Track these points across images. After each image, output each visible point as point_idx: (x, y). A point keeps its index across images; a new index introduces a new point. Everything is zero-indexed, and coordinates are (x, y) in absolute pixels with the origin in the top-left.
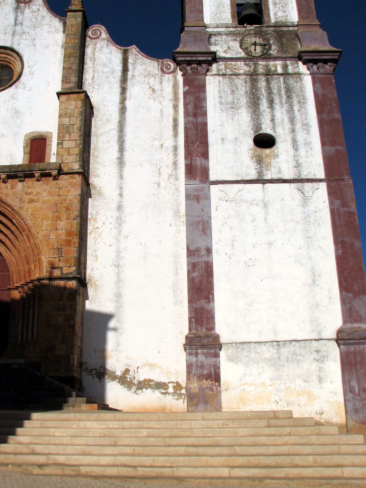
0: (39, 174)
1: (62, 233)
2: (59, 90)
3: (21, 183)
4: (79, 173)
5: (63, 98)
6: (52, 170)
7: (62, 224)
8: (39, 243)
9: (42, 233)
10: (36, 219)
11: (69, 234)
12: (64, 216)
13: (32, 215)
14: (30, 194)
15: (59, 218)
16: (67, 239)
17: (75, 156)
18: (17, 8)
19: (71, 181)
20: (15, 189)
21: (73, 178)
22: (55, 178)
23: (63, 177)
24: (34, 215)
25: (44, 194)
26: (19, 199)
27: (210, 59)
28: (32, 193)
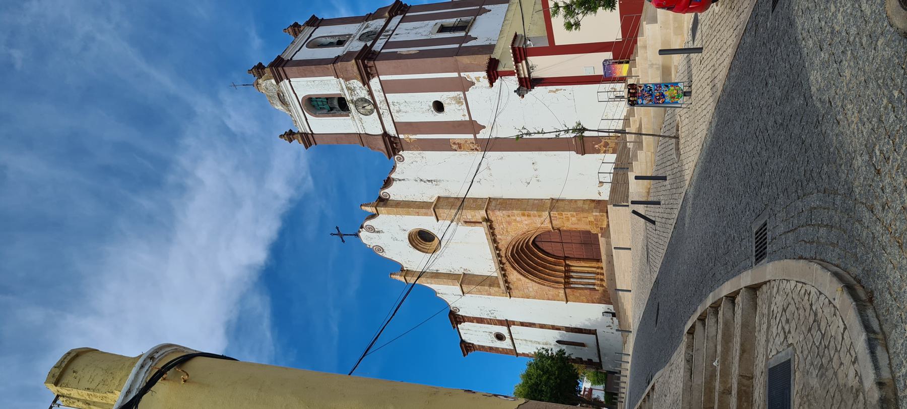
1: (523, 218)
2: (434, 218)
4: (486, 211)
5: (439, 218)
7: (518, 219)
9: (525, 227)
11: (524, 215)
12: (513, 218)
14: (503, 232)
15: (515, 220)
18: (378, 232)
21: (490, 214)
25: (502, 226)
27: (387, 138)
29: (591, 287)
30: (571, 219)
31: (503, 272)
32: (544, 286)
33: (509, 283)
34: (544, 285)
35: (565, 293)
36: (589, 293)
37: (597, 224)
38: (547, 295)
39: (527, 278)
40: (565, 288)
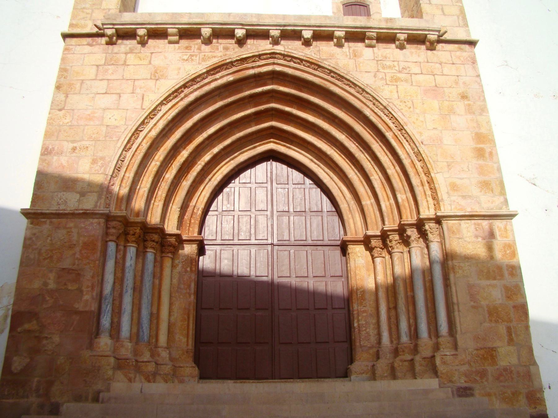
0: (406, 36)
3: (371, 49)
6: (429, 30)
8: (426, 151)
10: (411, 109)
13: (401, 102)
15: (452, 111)
16: (476, 148)
17: (456, 17)
19: (458, 53)
20: (362, 59)
22: (432, 47)
23: (443, 47)
24: (405, 102)
26: (373, 74)
28: (395, 66)
29: (106, 321)
30: (494, 286)
31: (206, 31)
32: (121, 145)
33: (143, 43)
34: (126, 149)
35: (86, 215)
36: (80, 306)
37: (483, 374)
38: (74, 149)
39: (167, 100)
40: (108, 218)
